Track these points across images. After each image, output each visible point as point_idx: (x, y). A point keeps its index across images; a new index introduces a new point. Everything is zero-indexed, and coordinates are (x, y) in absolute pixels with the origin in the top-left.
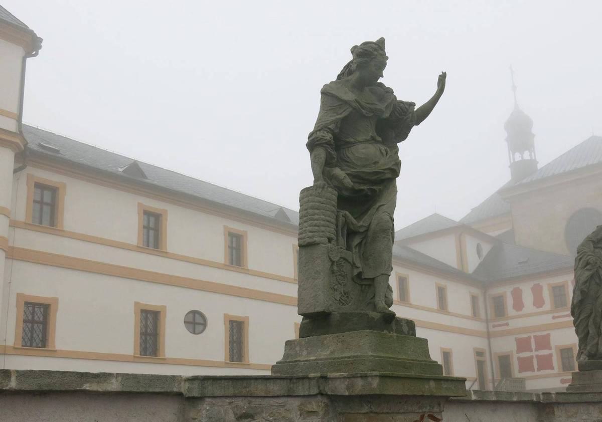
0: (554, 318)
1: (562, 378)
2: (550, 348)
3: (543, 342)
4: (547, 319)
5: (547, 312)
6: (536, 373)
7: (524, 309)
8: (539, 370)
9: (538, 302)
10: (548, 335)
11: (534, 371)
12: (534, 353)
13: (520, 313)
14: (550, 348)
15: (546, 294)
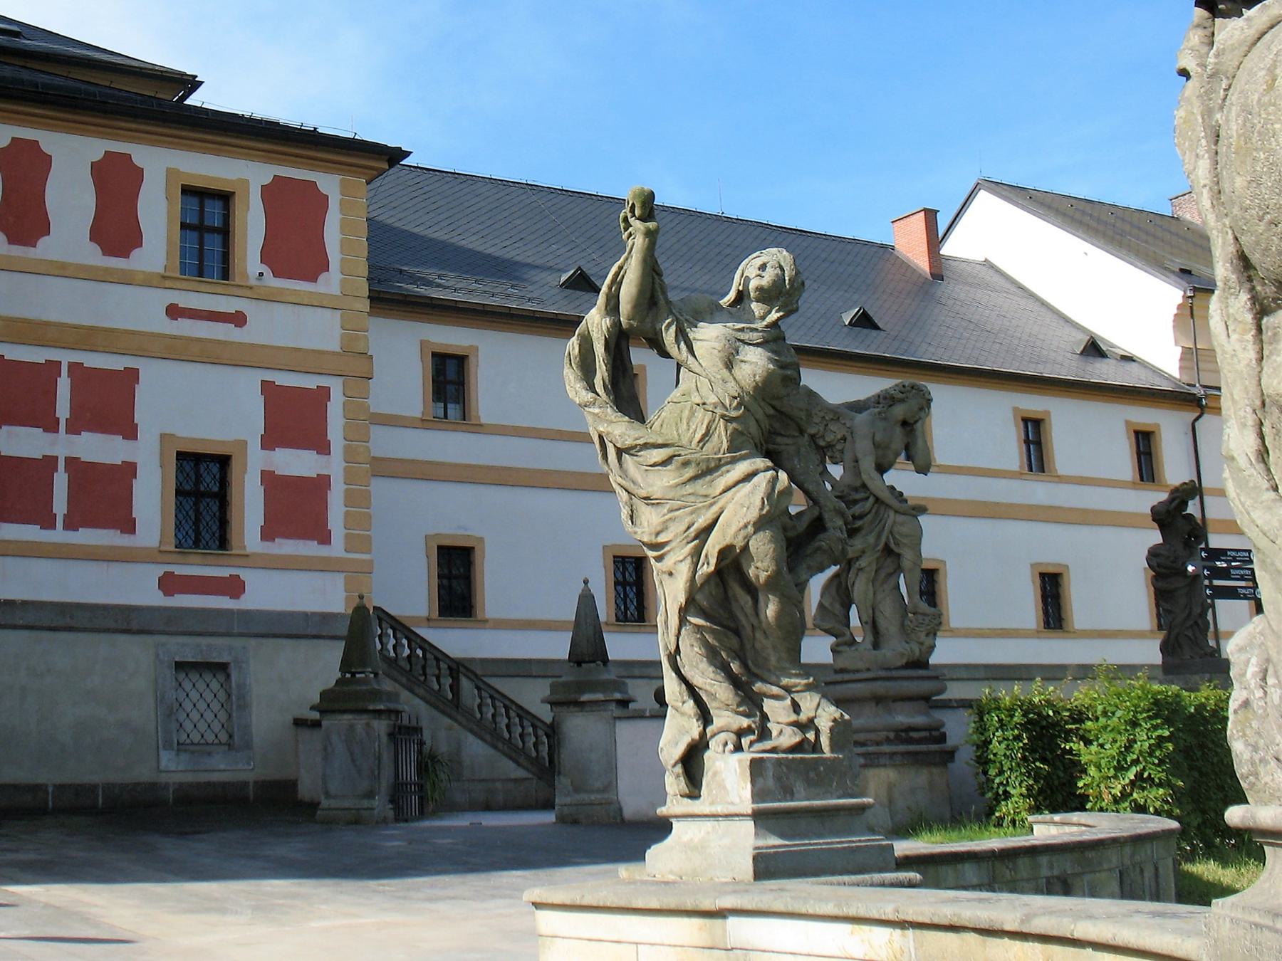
0: (174, 312)
1: (169, 568)
2: (130, 432)
3: (108, 404)
4: (142, 310)
5: (149, 281)
6: (59, 535)
7: (43, 242)
8: (70, 525)
9: (115, 229)
10: (132, 376)
11: (53, 527)
12: (63, 445)
13: (17, 251)
14: (130, 432)
15: (156, 213)
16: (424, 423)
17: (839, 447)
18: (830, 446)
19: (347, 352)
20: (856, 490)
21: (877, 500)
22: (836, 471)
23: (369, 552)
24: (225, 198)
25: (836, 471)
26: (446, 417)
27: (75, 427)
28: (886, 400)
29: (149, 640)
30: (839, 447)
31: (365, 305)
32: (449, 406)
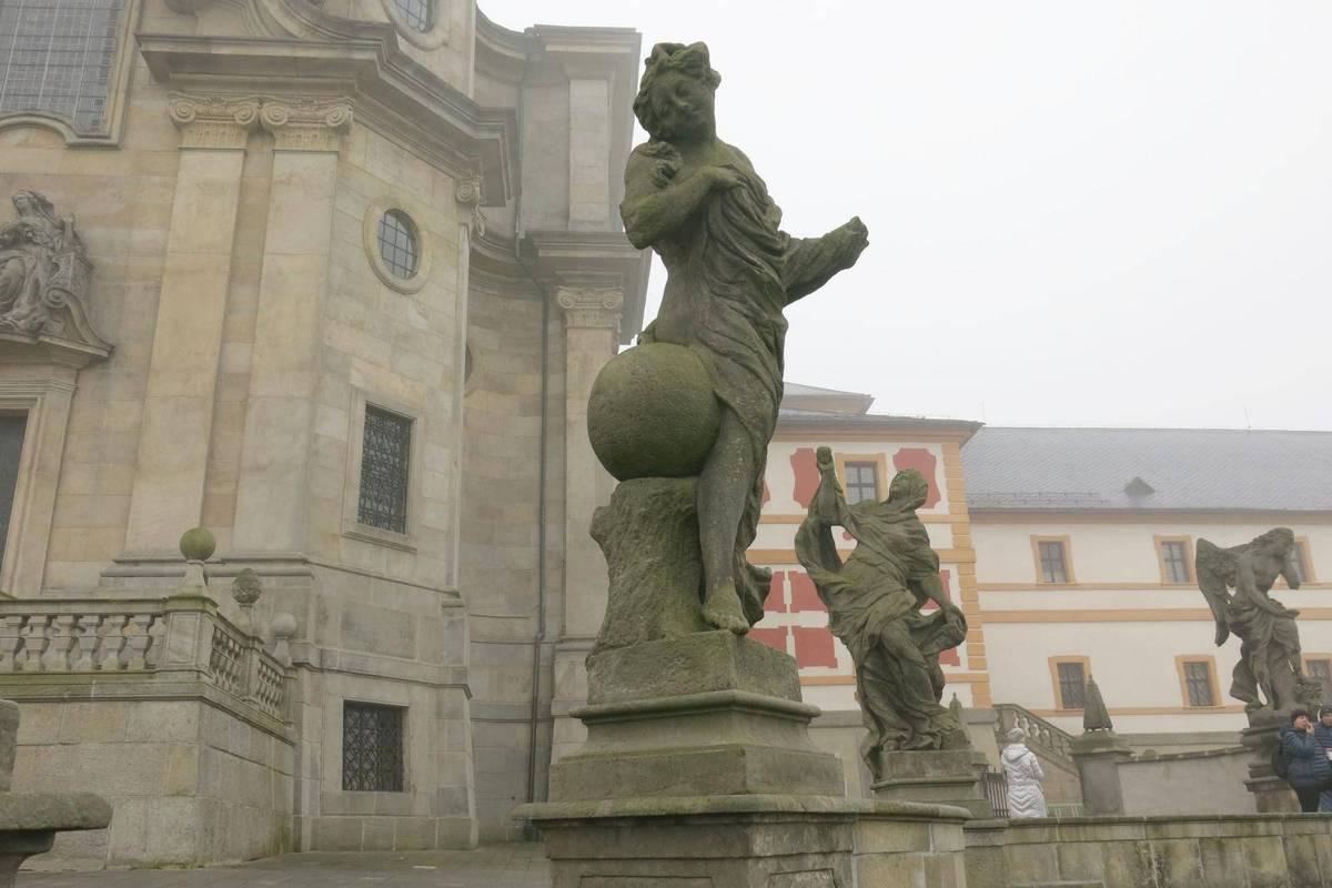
16: (1039, 587)
17: (1232, 576)
18: (1226, 576)
19: (957, 548)
20: (1244, 603)
21: (1261, 609)
22: (1232, 592)
23: (985, 669)
24: (872, 465)
25: (1232, 592)
26: (1053, 580)
27: (795, 609)
28: (1262, 542)
29: (851, 730)
30: (1232, 576)
31: (966, 518)
32: (1055, 574)
